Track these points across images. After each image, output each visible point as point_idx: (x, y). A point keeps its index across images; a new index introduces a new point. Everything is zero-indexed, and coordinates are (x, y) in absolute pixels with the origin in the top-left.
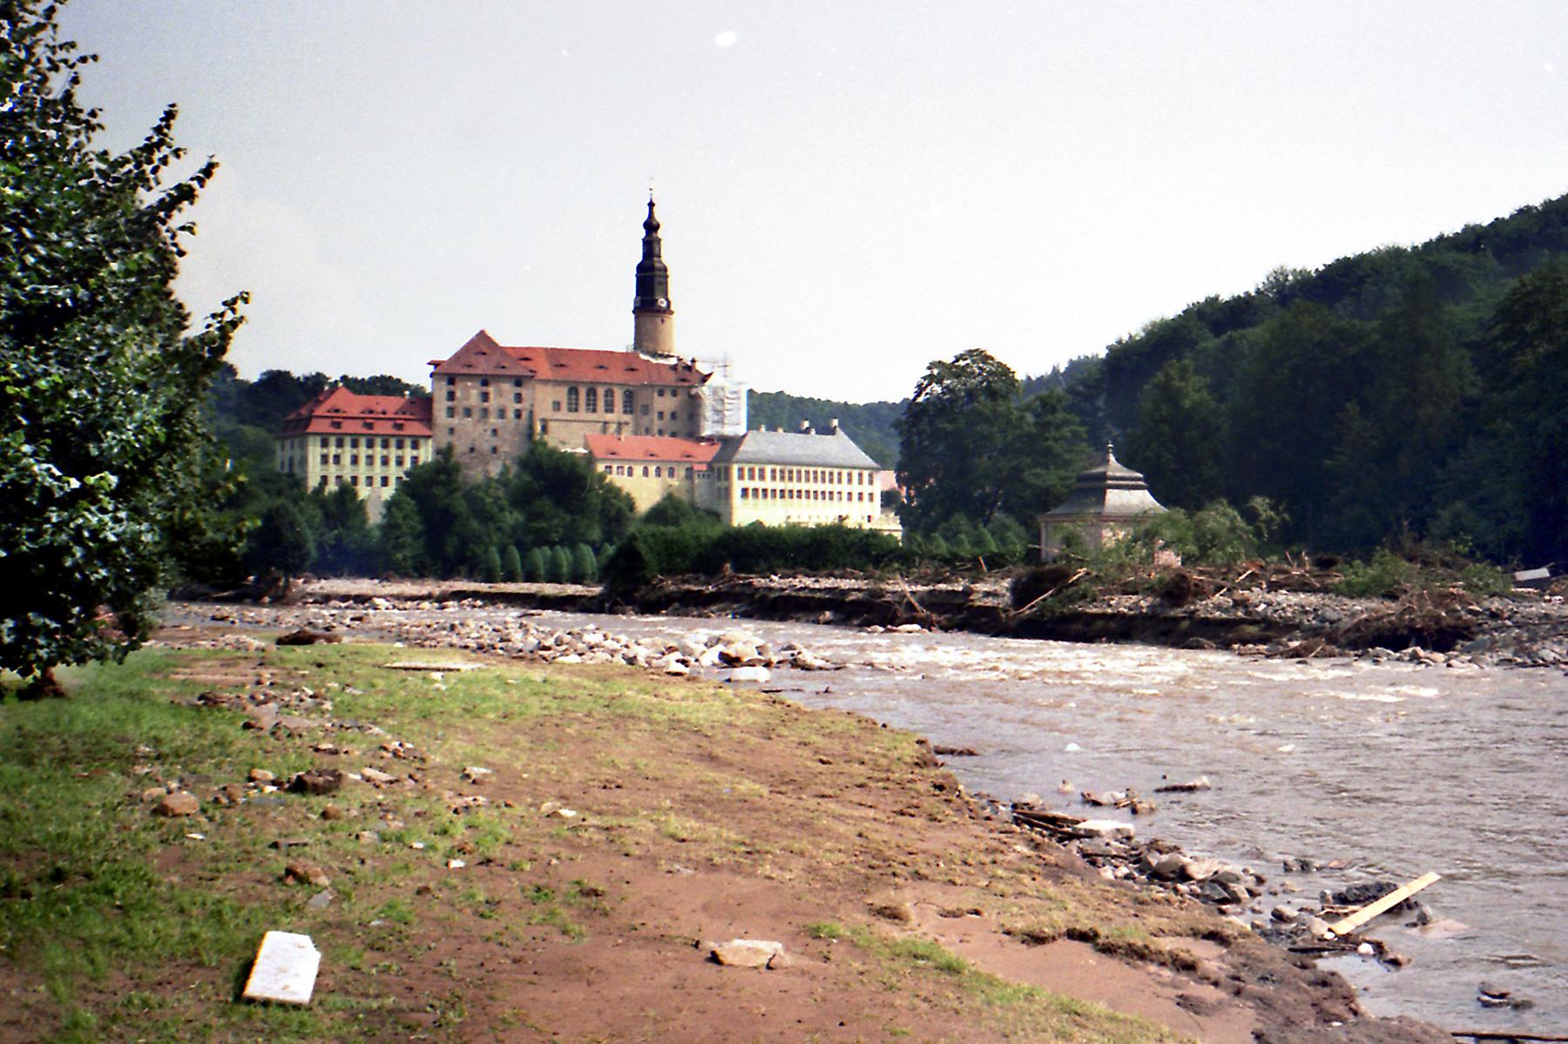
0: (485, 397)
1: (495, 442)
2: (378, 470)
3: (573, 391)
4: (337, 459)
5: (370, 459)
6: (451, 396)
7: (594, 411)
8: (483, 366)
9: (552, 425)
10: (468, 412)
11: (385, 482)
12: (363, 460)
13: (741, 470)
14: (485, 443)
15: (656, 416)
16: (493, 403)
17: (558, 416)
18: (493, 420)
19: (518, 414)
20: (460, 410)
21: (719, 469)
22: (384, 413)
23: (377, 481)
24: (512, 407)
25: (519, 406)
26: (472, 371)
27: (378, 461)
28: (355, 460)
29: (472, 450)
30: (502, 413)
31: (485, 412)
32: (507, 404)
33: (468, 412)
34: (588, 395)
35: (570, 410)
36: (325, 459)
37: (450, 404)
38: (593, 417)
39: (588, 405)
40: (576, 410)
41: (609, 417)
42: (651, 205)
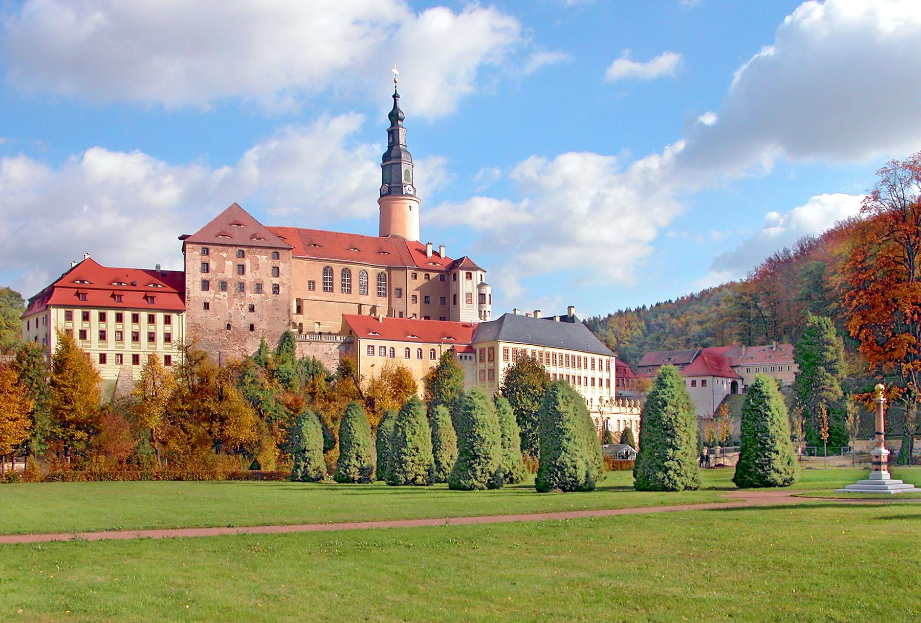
0: (242, 269)
1: (252, 318)
2: (128, 347)
3: (328, 271)
5: (120, 335)
6: (206, 268)
7: (349, 291)
8: (239, 236)
9: (306, 305)
10: (224, 286)
11: (136, 359)
12: (111, 335)
13: (506, 350)
14: (243, 319)
15: (410, 298)
16: (249, 277)
17: (311, 295)
18: (251, 296)
19: (276, 289)
20: (214, 284)
21: (482, 351)
22: (132, 284)
23: (128, 359)
25: (276, 281)
26: (227, 240)
27: (128, 337)
28: (103, 336)
30: (259, 288)
31: (242, 287)
32: (263, 277)
33: (224, 286)
34: (343, 275)
35: (325, 289)
38: (345, 297)
39: (343, 285)
40: (332, 290)
41: (363, 299)
42: (395, 96)
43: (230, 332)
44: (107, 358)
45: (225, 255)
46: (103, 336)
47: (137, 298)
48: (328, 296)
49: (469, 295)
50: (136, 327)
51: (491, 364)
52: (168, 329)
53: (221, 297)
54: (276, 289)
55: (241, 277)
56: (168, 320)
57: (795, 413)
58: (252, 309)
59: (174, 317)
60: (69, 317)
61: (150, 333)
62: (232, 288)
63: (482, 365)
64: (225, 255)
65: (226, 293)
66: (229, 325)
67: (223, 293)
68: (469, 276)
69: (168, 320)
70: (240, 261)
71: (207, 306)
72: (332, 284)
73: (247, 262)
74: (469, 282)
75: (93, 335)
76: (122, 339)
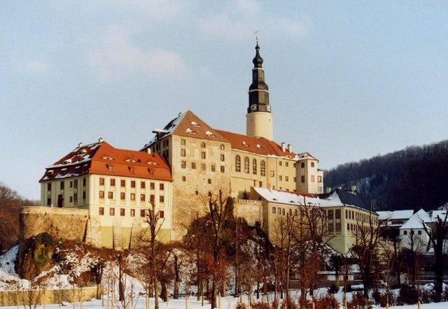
4: (111, 196)
5: (133, 196)
7: (248, 172)
12: (128, 196)
16: (208, 161)
19: (223, 169)
20: (189, 165)
24: (219, 164)
25: (223, 164)
27: (138, 198)
28: (123, 197)
29: (197, 193)
30: (213, 169)
33: (194, 166)
36: (102, 196)
37: (183, 158)
38: (246, 176)
39: (245, 168)
41: (255, 177)
42: (257, 48)
43: (197, 196)
44: (126, 212)
45: (194, 145)
46: (123, 197)
47: (144, 170)
48: (238, 174)
49: (313, 177)
50: (123, 190)
51: (338, 221)
52: (162, 193)
53: (192, 173)
54: (223, 169)
55: (204, 160)
56: (162, 187)
57: (324, 245)
58: (210, 181)
59: (166, 184)
60: (102, 182)
61: (161, 197)
62: (199, 167)
63: (331, 221)
64: (194, 145)
65: (195, 170)
66: (197, 193)
67: (193, 170)
68: (313, 165)
69: (162, 187)
70: (204, 150)
71: (184, 179)
72: (240, 167)
73: (206, 150)
74: (313, 168)
75: (117, 196)
76: (135, 199)
